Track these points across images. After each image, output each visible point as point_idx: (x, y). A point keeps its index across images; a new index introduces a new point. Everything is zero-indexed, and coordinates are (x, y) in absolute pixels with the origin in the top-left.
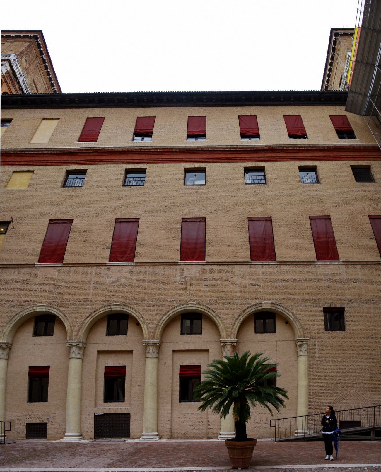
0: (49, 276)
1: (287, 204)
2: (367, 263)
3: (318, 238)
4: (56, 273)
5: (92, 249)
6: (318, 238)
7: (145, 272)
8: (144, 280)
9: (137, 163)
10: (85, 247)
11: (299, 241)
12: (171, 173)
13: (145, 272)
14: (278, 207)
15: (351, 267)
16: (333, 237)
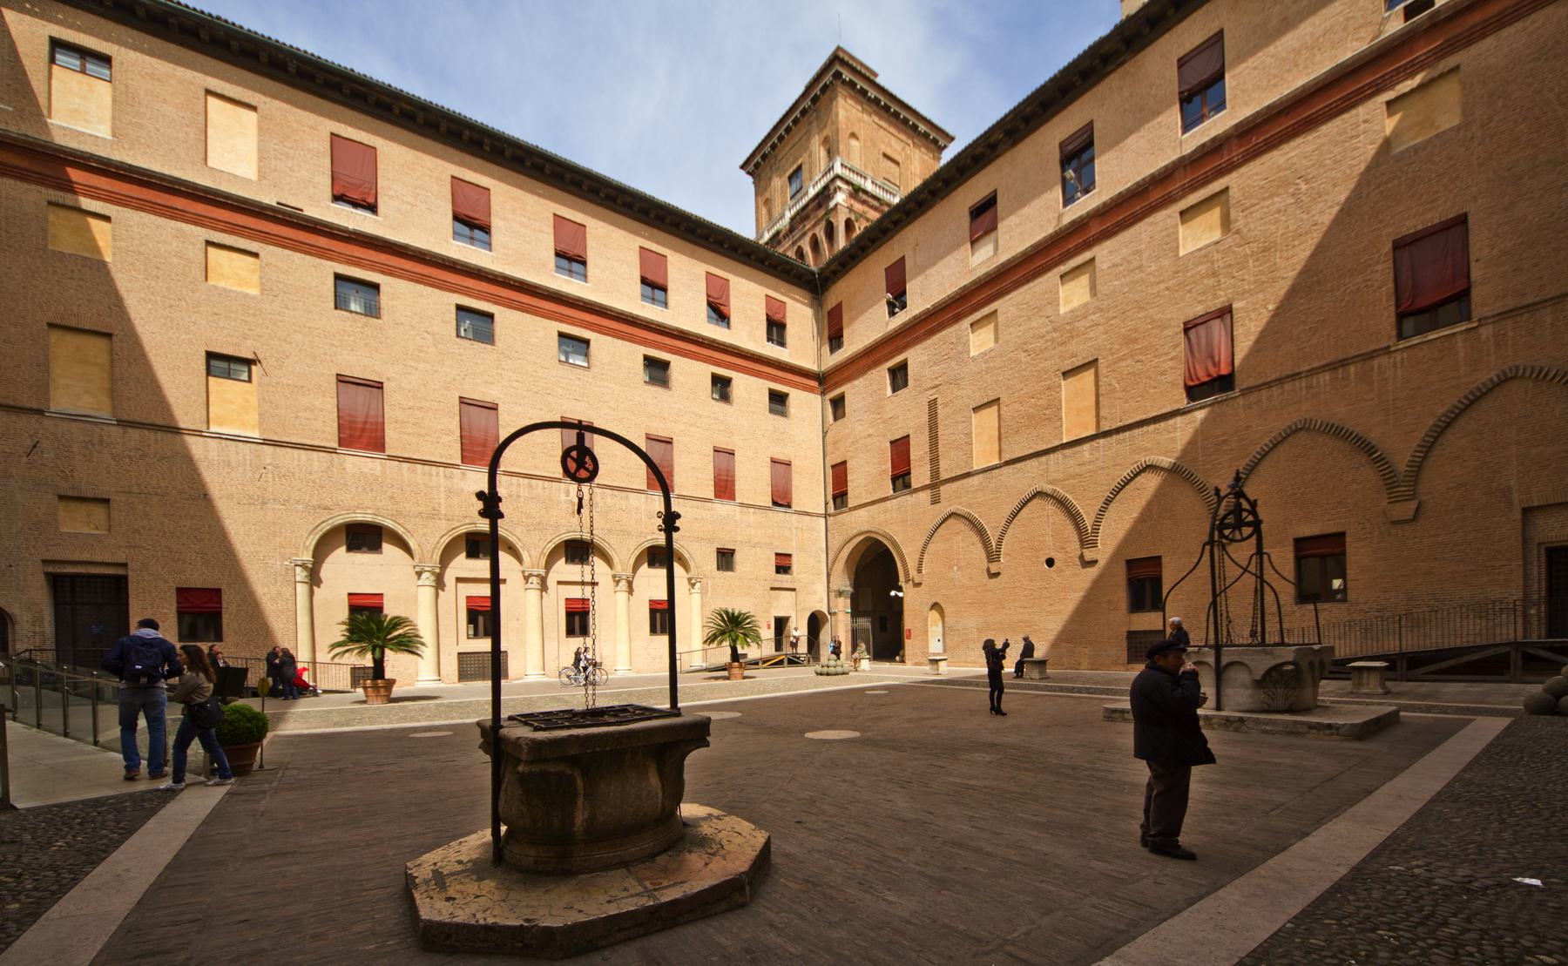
0: (365, 470)
1: (691, 425)
2: (760, 508)
3: (719, 475)
4: (379, 468)
5: (430, 439)
6: (719, 475)
7: (519, 485)
8: (519, 496)
9: (476, 298)
10: (419, 435)
11: (700, 475)
12: (538, 335)
13: (519, 485)
14: (682, 427)
15: (745, 509)
16: (734, 476)
